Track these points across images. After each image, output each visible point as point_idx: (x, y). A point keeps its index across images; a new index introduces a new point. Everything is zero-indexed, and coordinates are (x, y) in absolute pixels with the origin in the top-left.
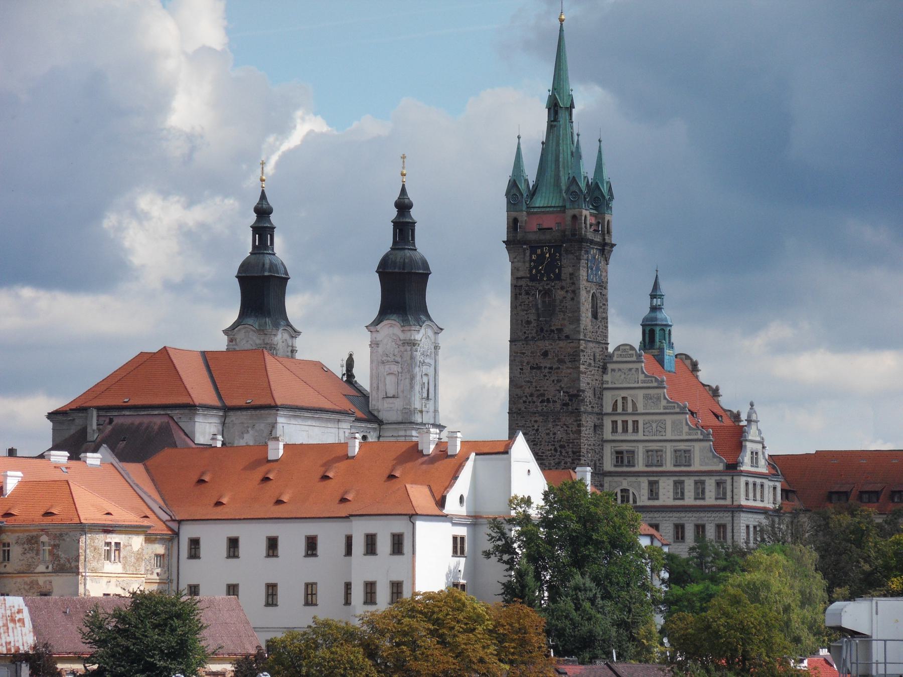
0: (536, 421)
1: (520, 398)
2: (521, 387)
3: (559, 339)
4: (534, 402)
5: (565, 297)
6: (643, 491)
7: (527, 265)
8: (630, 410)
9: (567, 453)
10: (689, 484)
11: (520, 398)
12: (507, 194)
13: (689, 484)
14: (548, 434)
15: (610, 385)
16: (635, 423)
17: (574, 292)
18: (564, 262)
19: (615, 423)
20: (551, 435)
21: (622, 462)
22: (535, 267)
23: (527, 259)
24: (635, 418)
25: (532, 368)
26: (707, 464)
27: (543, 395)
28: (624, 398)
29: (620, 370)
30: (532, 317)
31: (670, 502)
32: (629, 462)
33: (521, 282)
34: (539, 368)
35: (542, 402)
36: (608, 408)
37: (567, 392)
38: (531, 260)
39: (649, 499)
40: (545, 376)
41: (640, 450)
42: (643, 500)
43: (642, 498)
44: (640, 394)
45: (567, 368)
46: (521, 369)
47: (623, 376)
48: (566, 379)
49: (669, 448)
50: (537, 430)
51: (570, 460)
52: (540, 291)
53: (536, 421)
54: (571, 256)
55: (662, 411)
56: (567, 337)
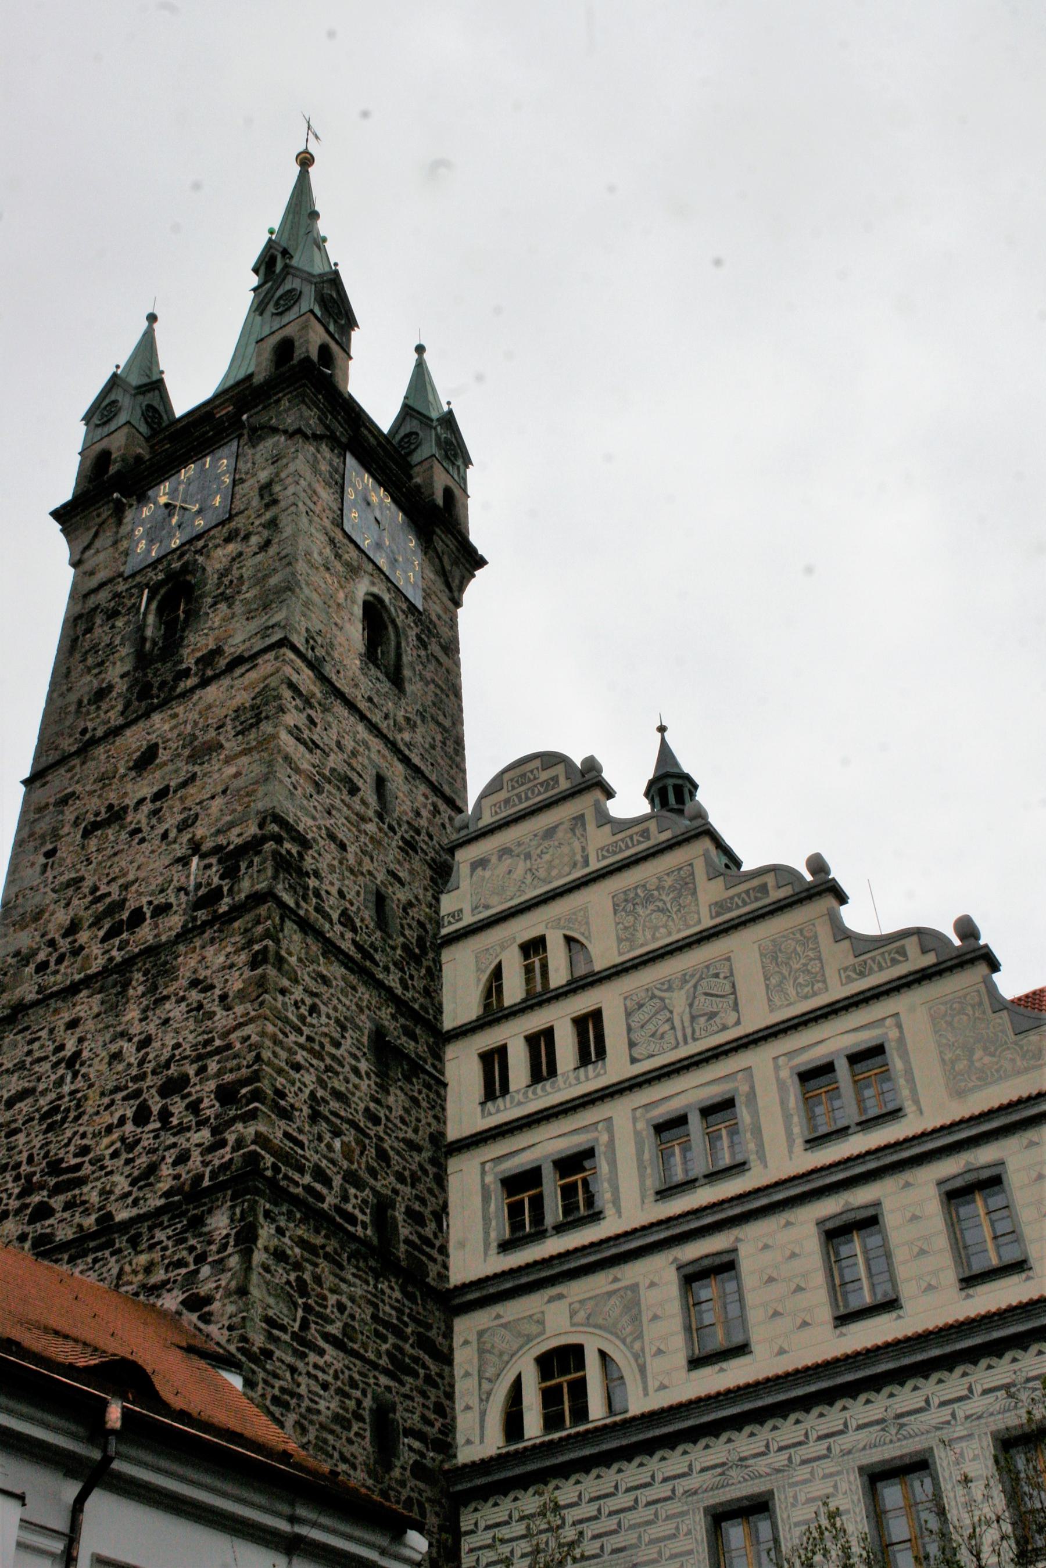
0: (73, 1024)
3: (205, 683)
4: (77, 951)
5: (240, 554)
6: (652, 1332)
9: (194, 1107)
10: (909, 1204)
12: (87, 418)
13: (909, 1204)
15: (468, 919)
16: (588, 1026)
17: (273, 524)
19: (494, 1061)
21: (538, 1216)
24: (582, 1003)
26: (985, 1079)
28: (534, 947)
29: (505, 852)
31: (826, 1343)
32: (568, 1209)
33: (103, 597)
36: (460, 999)
37: (218, 849)
39: (695, 1363)
40: (138, 831)
41: (621, 1137)
42: (659, 1377)
43: (654, 1365)
44: (597, 899)
45: (228, 761)
47: (521, 866)
49: (768, 1073)
50: (73, 1061)
51: (204, 1135)
53: (73, 1024)
55: (707, 922)
56: (238, 661)
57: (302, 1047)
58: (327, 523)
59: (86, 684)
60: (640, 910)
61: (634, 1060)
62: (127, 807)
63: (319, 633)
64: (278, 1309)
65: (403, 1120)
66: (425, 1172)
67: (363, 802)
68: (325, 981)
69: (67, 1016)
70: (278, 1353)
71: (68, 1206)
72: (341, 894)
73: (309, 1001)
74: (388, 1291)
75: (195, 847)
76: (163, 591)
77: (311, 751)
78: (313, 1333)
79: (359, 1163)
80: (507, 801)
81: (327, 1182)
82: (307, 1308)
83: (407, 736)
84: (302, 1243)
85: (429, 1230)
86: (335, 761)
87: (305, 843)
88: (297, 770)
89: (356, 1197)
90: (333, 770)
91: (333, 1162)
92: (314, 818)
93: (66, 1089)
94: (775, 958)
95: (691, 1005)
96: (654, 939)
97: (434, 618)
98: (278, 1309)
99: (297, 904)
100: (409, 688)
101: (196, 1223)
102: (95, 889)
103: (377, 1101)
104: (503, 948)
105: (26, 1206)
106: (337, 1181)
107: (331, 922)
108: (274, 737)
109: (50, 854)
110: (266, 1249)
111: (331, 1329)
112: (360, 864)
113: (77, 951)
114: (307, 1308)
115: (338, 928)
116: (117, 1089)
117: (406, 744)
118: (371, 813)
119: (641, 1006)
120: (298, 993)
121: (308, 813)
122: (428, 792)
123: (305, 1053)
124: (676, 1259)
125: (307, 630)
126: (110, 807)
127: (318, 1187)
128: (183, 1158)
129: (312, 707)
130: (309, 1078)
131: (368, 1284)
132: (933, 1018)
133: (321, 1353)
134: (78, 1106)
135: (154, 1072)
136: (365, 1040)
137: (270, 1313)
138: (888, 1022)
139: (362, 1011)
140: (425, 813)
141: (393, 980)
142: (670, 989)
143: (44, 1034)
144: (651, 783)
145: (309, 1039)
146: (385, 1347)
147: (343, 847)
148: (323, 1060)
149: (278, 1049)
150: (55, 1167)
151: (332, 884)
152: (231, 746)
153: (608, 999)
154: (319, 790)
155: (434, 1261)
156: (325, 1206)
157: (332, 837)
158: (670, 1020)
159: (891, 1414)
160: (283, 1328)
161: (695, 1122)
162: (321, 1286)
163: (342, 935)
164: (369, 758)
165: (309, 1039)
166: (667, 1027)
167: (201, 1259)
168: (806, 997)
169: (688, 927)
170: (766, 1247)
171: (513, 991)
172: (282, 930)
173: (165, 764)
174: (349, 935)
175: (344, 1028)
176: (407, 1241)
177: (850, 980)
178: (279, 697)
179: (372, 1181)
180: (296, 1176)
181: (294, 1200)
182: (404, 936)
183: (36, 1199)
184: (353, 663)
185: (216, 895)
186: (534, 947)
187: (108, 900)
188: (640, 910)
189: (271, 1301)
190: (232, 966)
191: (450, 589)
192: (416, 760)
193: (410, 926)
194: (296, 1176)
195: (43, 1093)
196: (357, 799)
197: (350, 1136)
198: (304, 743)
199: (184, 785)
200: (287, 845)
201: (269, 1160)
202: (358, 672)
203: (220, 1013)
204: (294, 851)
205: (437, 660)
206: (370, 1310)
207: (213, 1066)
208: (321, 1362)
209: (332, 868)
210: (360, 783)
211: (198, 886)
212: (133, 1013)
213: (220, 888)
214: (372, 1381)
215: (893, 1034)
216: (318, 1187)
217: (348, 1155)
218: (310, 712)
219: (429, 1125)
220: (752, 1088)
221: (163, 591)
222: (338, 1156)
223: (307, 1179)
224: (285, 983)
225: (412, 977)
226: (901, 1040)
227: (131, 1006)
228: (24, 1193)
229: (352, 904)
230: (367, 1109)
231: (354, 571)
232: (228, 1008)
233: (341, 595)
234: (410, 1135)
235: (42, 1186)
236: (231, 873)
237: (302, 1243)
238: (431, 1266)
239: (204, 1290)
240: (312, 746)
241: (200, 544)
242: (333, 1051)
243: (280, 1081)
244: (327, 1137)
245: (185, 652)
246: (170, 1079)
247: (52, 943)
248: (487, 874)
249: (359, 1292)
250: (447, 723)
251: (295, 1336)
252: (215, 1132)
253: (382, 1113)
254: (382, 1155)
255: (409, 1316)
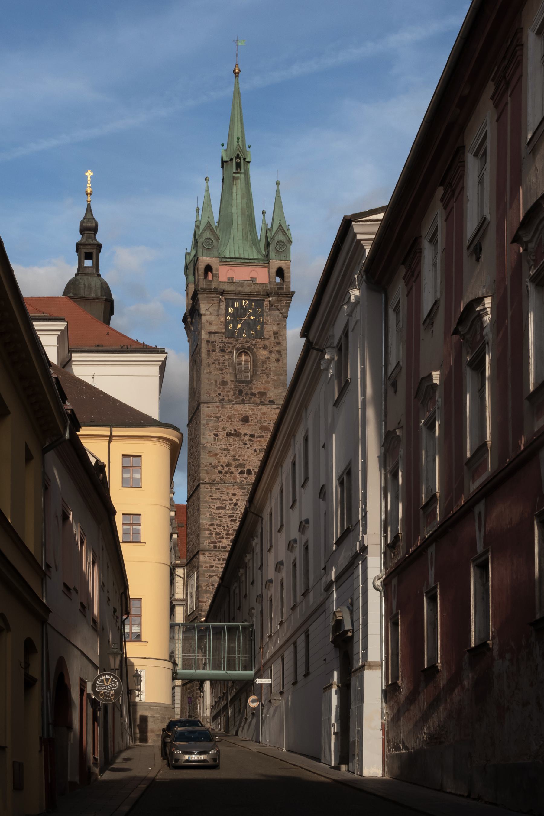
0: (234, 494)
1: (215, 467)
2: (216, 455)
3: (263, 403)
5: (268, 358)
7: (223, 319)
11: (215, 467)
17: (279, 352)
18: (267, 319)
22: (231, 321)
23: (224, 312)
25: (229, 435)
27: (241, 465)
30: (229, 378)
34: (237, 434)
35: (242, 473)
38: (227, 314)
46: (216, 435)
50: (236, 504)
52: (238, 350)
53: (234, 494)
54: (276, 313)
62: (241, 434)
126: (235, 431)
173: (252, 425)
187: (240, 462)
195: (228, 510)
247: (222, 466)
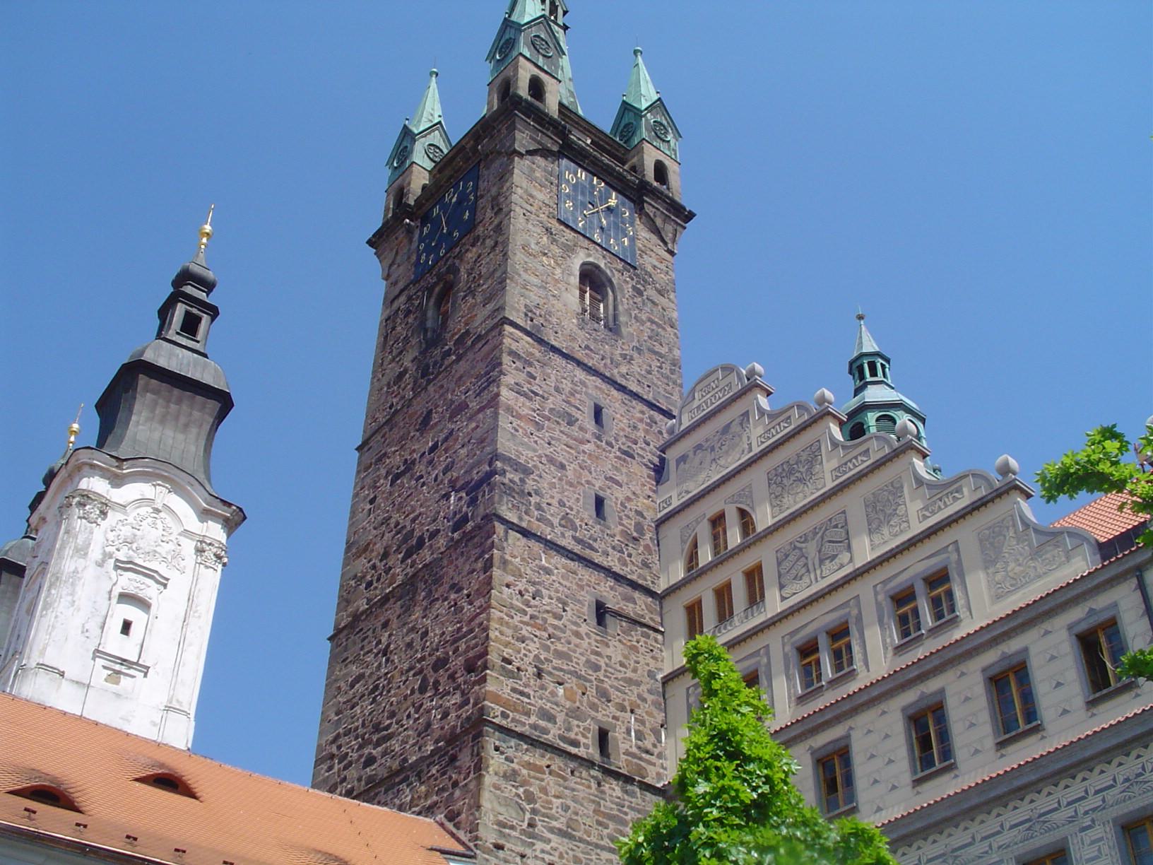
0: (385, 625)
8: (734, 537)
11: (359, 580)
14: (409, 645)
20: (417, 644)
29: (699, 447)
40: (421, 477)
45: (470, 419)
46: (372, 502)
48: (463, 452)
51: (457, 698)
53: (385, 625)
55: (830, 485)
57: (526, 624)
58: (543, 217)
59: (393, 370)
60: (785, 481)
61: (783, 599)
63: (537, 306)
64: (509, 815)
65: (622, 665)
66: (644, 700)
67: (581, 429)
68: (548, 572)
69: (383, 619)
70: (508, 845)
71: (384, 754)
72: (562, 504)
73: (532, 589)
74: (609, 792)
75: (452, 483)
76: (437, 289)
77: (530, 399)
78: (540, 828)
79: (581, 702)
80: (698, 407)
81: (551, 718)
82: (534, 811)
83: (624, 370)
84: (529, 765)
85: (648, 744)
86: (554, 402)
87: (527, 471)
88: (519, 417)
89: (578, 726)
90: (551, 410)
91: (557, 704)
92: (535, 450)
93: (383, 671)
94: (875, 507)
95: (820, 551)
96: (795, 502)
97: (649, 269)
98: (509, 815)
99: (521, 519)
100: (624, 330)
101: (454, 759)
102: (397, 524)
103: (598, 654)
104: (698, 523)
105: (361, 756)
106: (560, 718)
107: (552, 526)
108: (498, 395)
109: (372, 502)
110: (496, 774)
111: (554, 824)
112: (580, 477)
113: (388, 570)
114: (534, 811)
115: (558, 530)
116: (410, 669)
117: (623, 376)
118: (588, 436)
119: (787, 556)
120: (521, 585)
121: (529, 448)
122: (645, 408)
123: (529, 628)
124: (811, 747)
125: (526, 306)
127: (542, 723)
128: (445, 715)
129: (531, 365)
130: (533, 647)
131: (589, 787)
132: (981, 541)
133: (549, 841)
134: (389, 683)
135: (430, 655)
136: (585, 609)
137: (501, 818)
138: (950, 548)
139: (582, 587)
140: (641, 426)
141: (612, 562)
142: (806, 541)
143: (370, 633)
144: (851, 364)
145: (532, 617)
146: (606, 832)
147: (563, 467)
148: (545, 630)
149: (504, 629)
150: (377, 728)
151: (552, 497)
152: (474, 405)
153: (765, 555)
154: (539, 427)
155: (654, 764)
156: (550, 737)
157: (551, 461)
158: (806, 565)
159: (949, 848)
160: (512, 828)
161: (823, 642)
162: (547, 794)
163: (563, 535)
164: (586, 393)
165: (532, 617)
166: (804, 570)
167: (455, 784)
168: (896, 535)
169: (818, 490)
170: (869, 731)
171: (706, 555)
172: (506, 540)
173: (436, 424)
174: (569, 533)
175: (565, 604)
176: (627, 753)
177: (925, 517)
178: (500, 364)
179: (593, 713)
180: (523, 719)
181: (521, 737)
182: (621, 524)
183: (366, 751)
184: (571, 324)
185: (465, 519)
186: (718, 521)
188: (785, 481)
189: (502, 810)
190: (474, 571)
191: (665, 243)
192: (634, 387)
193: (628, 517)
194: (523, 719)
196: (575, 428)
197: (572, 682)
198: (525, 395)
199: (446, 439)
200: (509, 475)
201: (498, 709)
202: (575, 329)
203: (467, 607)
204: (517, 479)
205: (653, 302)
206: (593, 807)
207: (463, 647)
208: (548, 847)
209: (553, 486)
210: (577, 414)
211: (455, 513)
212: (418, 613)
213: (466, 514)
214: (594, 857)
215: (954, 557)
216: (542, 723)
217: (570, 696)
218: (528, 369)
219: (648, 665)
220: (860, 612)
221: (437, 289)
222: (563, 701)
223: (533, 719)
224: (510, 579)
225: (630, 555)
226: (959, 562)
227: (417, 608)
228: (361, 747)
229: (571, 509)
230: (588, 661)
231: (569, 250)
232: (471, 603)
233: (558, 271)
234: (629, 674)
235: (369, 742)
236: (473, 502)
237: (529, 765)
238: (649, 768)
239: (456, 807)
240: (531, 395)
241: (458, 250)
242: (556, 622)
243: (507, 652)
244: (551, 686)
245: (448, 336)
246: (438, 659)
248: (687, 466)
249: (581, 795)
250: (664, 350)
251: (523, 832)
252: (463, 694)
253: (602, 663)
254: (604, 695)
255: (629, 807)
